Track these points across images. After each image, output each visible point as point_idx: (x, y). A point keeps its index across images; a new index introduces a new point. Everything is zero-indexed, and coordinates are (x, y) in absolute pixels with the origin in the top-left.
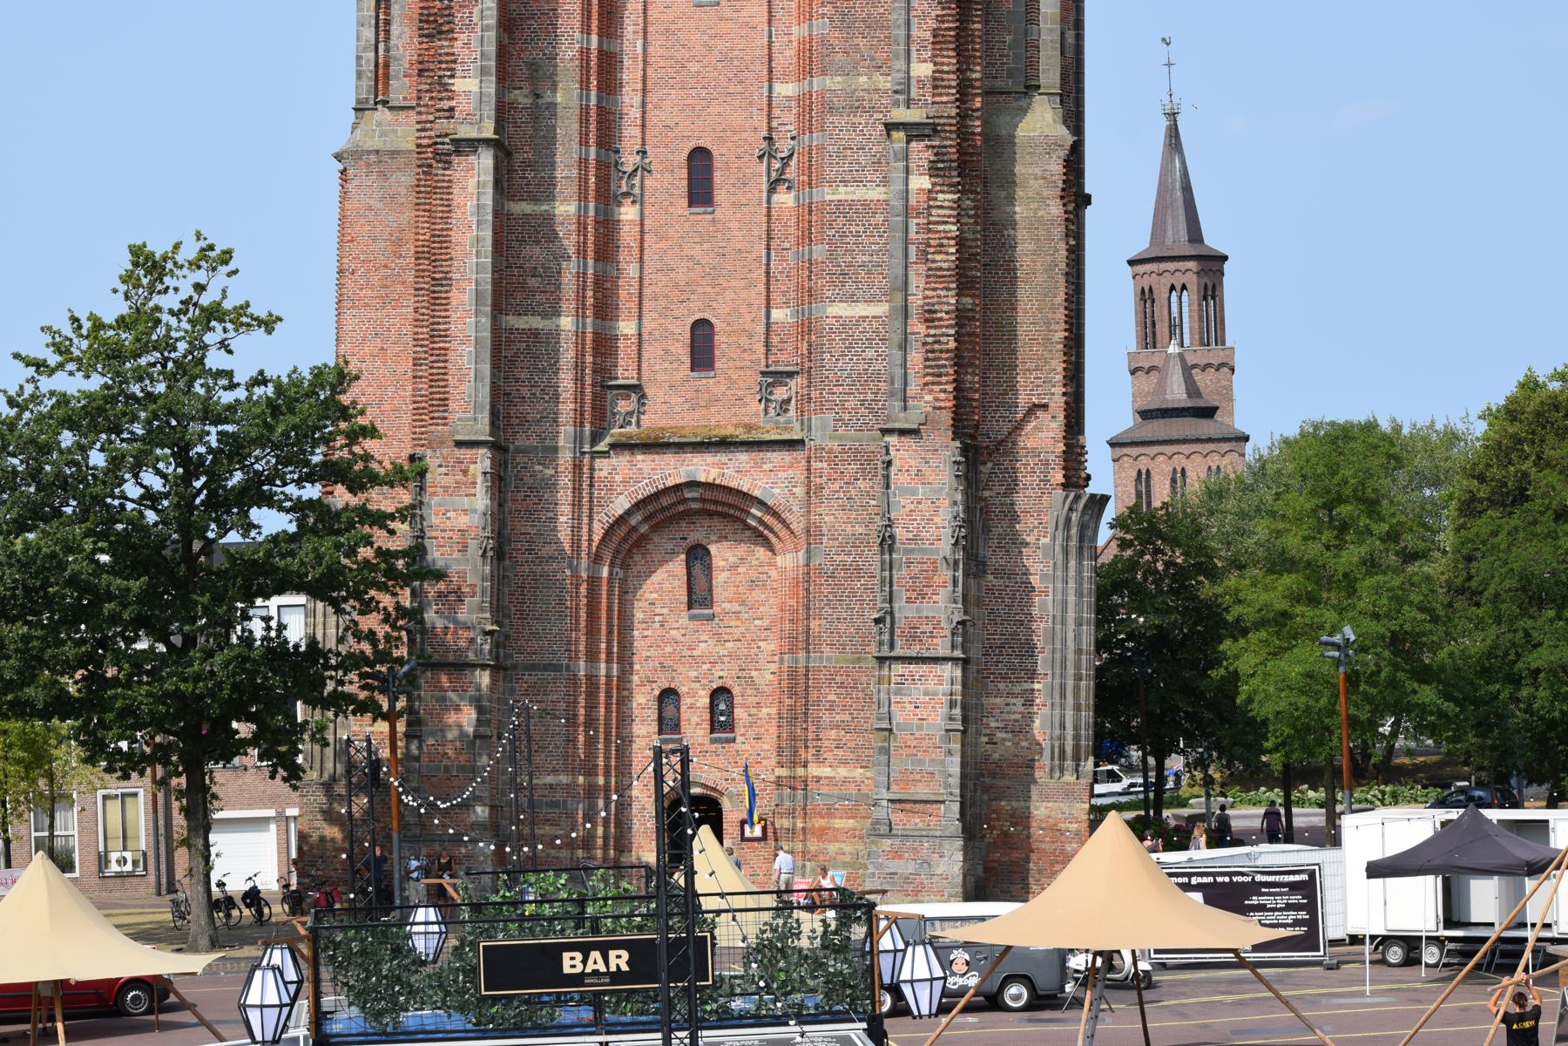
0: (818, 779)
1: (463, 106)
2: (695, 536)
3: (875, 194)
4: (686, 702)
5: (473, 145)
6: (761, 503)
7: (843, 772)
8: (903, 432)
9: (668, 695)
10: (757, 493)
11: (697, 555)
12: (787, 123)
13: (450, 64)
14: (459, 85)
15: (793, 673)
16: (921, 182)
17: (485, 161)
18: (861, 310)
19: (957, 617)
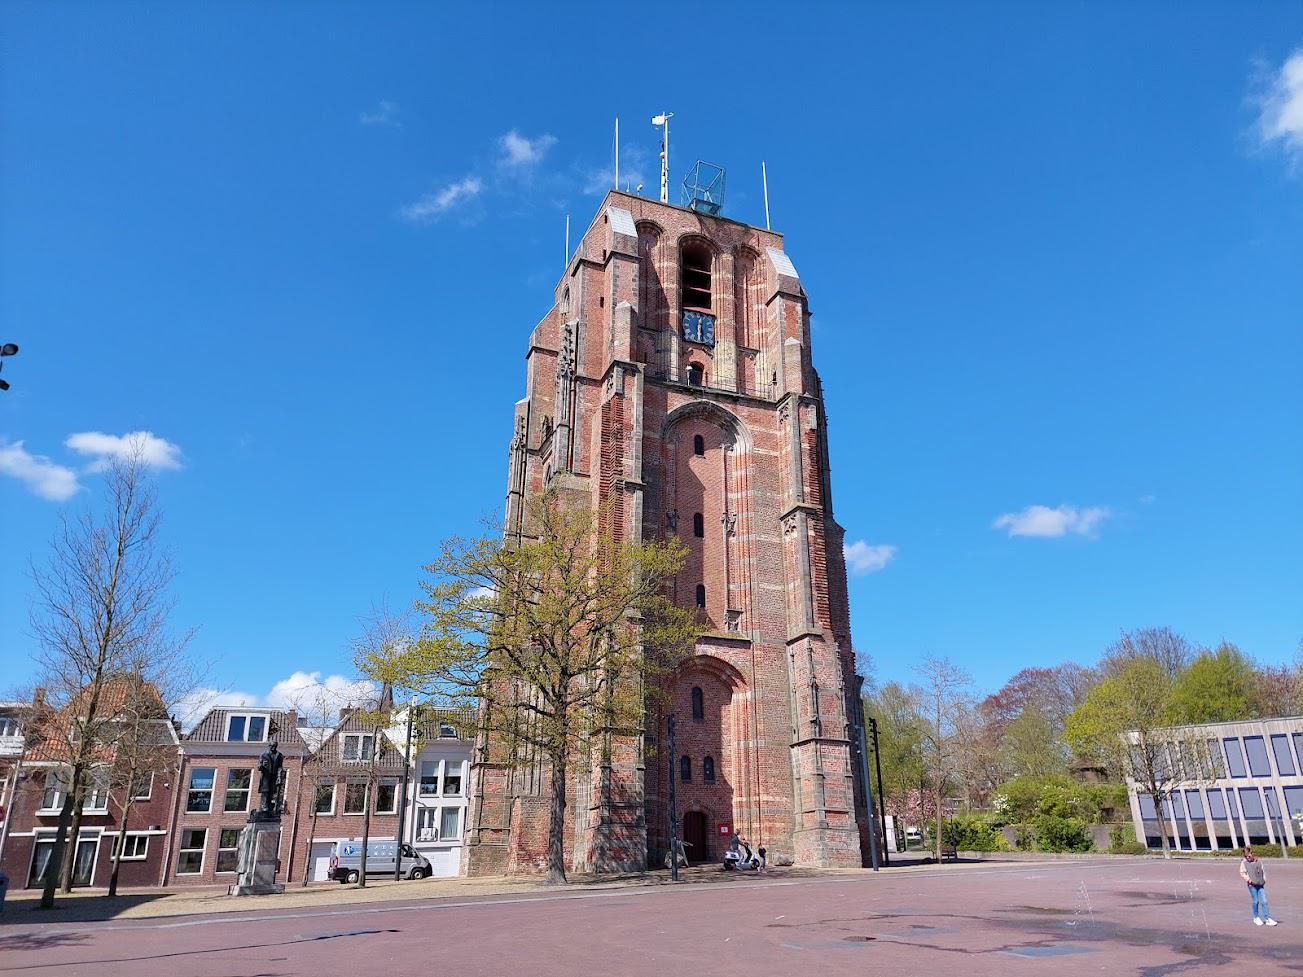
0: (767, 802)
1: (625, 469)
2: (696, 683)
3: (776, 540)
4: (693, 762)
5: (631, 487)
6: (732, 668)
7: (777, 799)
8: (816, 636)
9: (686, 760)
10: (731, 663)
11: (697, 693)
12: (733, 510)
13: (620, 452)
14: (624, 461)
15: (747, 750)
16: (812, 533)
17: (639, 494)
18: (772, 587)
19: (846, 722)
